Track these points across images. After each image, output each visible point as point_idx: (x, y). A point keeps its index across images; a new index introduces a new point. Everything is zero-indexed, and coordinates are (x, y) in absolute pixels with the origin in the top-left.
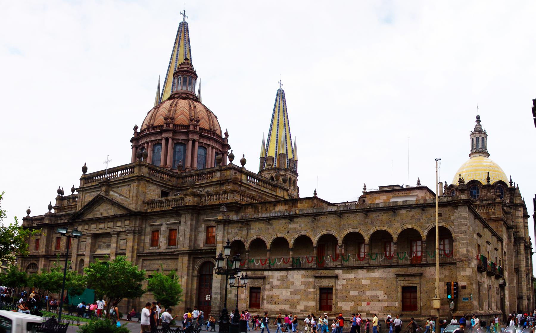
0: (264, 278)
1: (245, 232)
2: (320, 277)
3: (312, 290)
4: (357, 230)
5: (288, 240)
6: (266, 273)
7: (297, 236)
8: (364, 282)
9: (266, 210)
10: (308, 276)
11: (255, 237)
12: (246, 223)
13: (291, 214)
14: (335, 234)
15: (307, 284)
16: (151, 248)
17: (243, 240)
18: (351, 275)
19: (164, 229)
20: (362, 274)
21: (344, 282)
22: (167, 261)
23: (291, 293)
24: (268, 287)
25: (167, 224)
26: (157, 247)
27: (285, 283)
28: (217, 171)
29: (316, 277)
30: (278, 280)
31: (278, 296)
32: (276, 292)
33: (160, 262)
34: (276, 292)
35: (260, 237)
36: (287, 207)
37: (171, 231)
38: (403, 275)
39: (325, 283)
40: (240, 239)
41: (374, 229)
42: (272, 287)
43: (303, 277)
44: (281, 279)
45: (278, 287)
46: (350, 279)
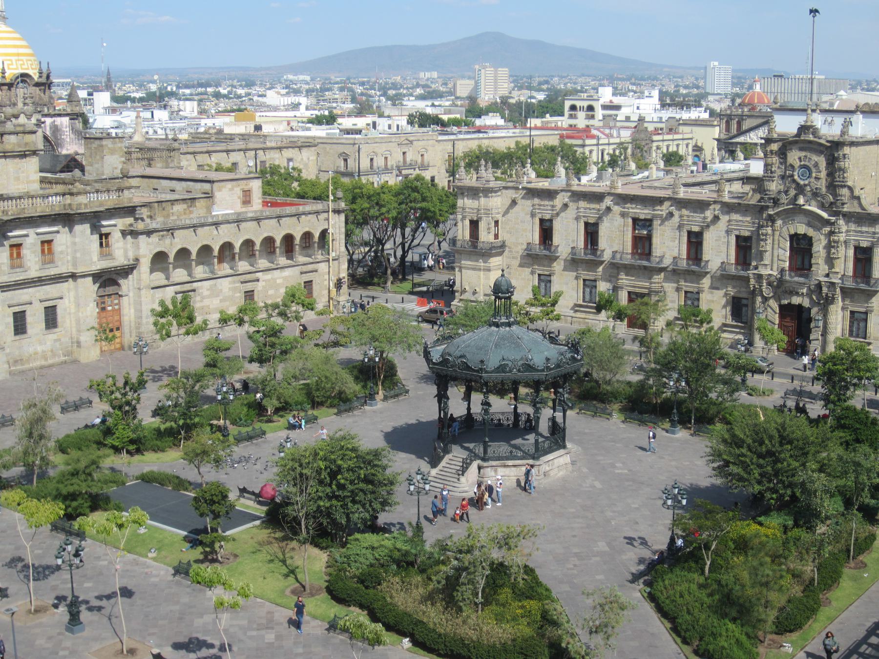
0: (194, 291)
1: (168, 241)
2: (246, 282)
3: (238, 294)
4: (271, 234)
5: (213, 247)
6: (195, 285)
7: (221, 243)
8: (278, 281)
9: (164, 209)
10: (234, 282)
11: (179, 247)
12: (171, 231)
13: (215, 220)
14: (253, 239)
15: (234, 290)
16: (12, 271)
17: (166, 251)
18: (268, 276)
19: (32, 241)
20: (276, 273)
21: (264, 283)
22: (44, 287)
23: (221, 301)
24: (198, 298)
25: (38, 234)
26: (21, 270)
27: (215, 293)
28: (10, 133)
29: (242, 283)
30: (208, 290)
31: (208, 307)
32: (206, 302)
33: (30, 289)
34: (206, 302)
35: (184, 246)
36: (185, 206)
37: (43, 242)
38: (306, 273)
39: (249, 287)
40: (163, 249)
41: (283, 233)
42: (203, 298)
43: (230, 283)
44: (211, 289)
45: (209, 297)
46: (269, 280)
